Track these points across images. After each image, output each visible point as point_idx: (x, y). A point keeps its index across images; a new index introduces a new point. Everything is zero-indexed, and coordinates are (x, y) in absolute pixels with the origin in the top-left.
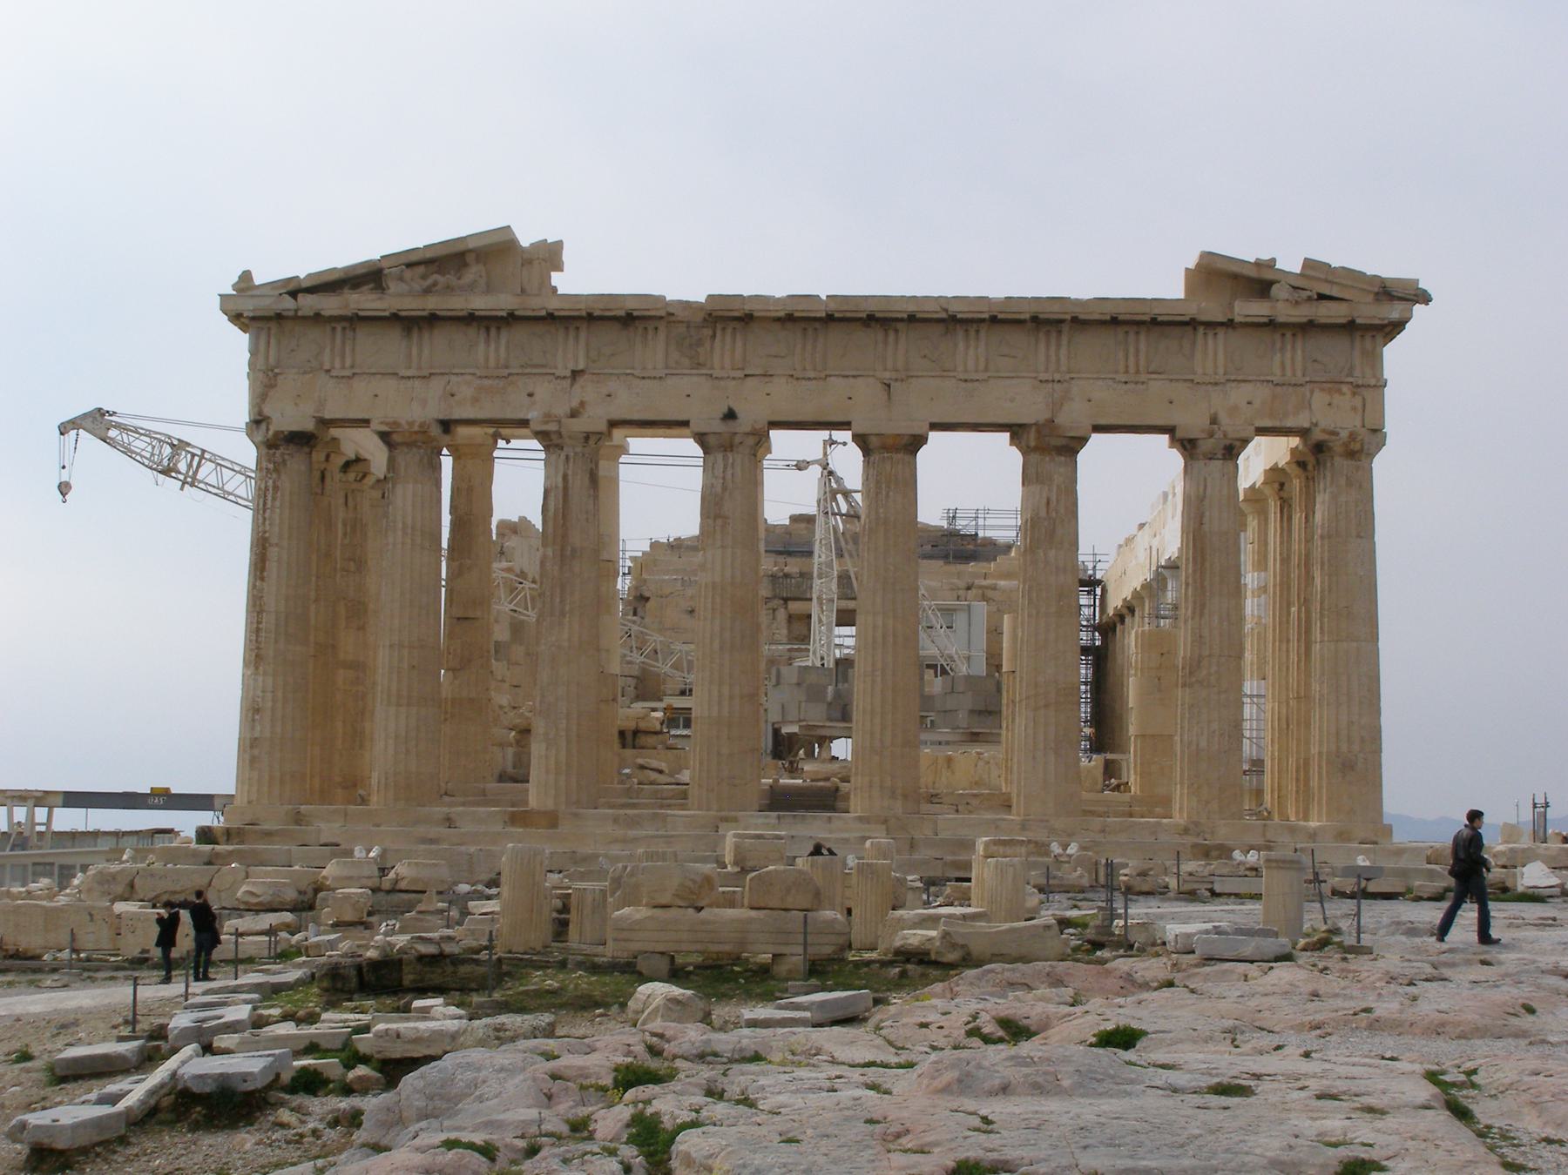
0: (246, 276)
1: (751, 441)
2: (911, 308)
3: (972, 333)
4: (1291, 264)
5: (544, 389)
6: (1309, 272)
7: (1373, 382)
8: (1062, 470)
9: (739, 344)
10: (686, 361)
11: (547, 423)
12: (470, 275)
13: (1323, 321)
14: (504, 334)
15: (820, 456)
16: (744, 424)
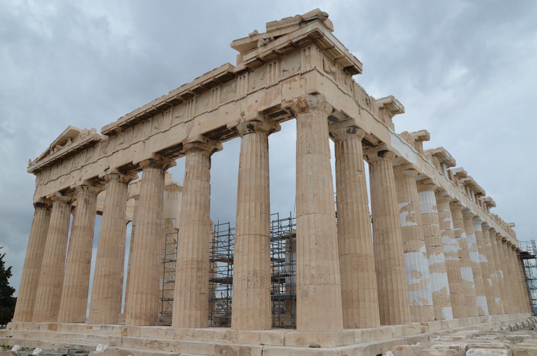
0: (30, 161)
1: (115, 177)
6: (269, 29)
16: (109, 171)
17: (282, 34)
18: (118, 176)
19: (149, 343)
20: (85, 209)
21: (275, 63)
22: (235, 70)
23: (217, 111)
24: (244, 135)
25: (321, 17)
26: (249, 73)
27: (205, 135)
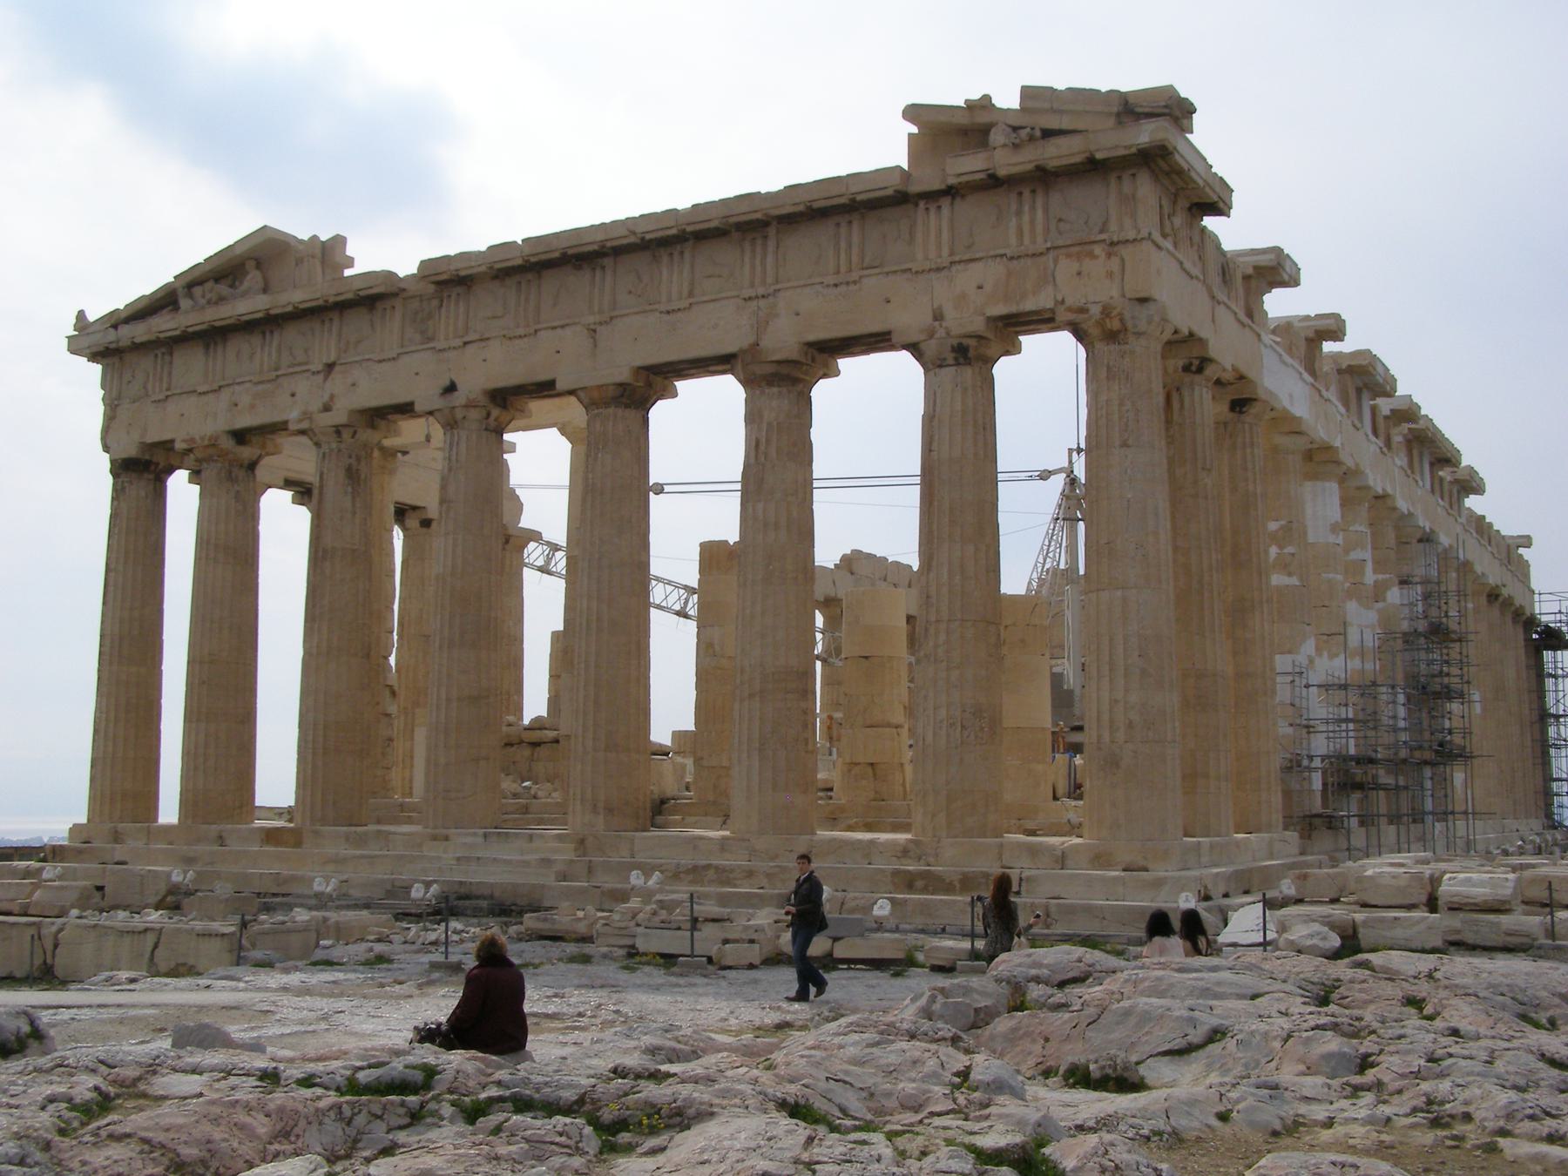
0: (81, 315)
1: (475, 414)
2: (600, 237)
3: (676, 256)
4: (1007, 99)
5: (302, 386)
6: (1030, 104)
7: (1131, 235)
8: (774, 403)
9: (462, 309)
10: (418, 337)
11: (300, 421)
12: (246, 284)
13: (1052, 164)
14: (276, 335)
15: (1066, 465)
17: (1064, 126)
18: (484, 413)
19: (688, 872)
20: (349, 497)
21: (1033, 191)
22: (914, 188)
23: (852, 287)
24: (940, 366)
25: (1176, 110)
26: (953, 198)
27: (810, 345)
